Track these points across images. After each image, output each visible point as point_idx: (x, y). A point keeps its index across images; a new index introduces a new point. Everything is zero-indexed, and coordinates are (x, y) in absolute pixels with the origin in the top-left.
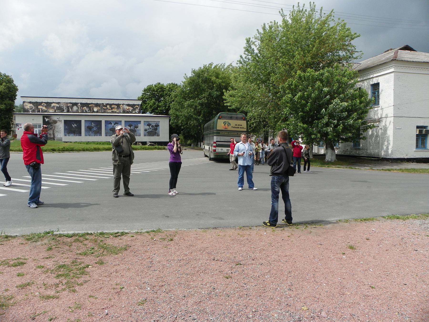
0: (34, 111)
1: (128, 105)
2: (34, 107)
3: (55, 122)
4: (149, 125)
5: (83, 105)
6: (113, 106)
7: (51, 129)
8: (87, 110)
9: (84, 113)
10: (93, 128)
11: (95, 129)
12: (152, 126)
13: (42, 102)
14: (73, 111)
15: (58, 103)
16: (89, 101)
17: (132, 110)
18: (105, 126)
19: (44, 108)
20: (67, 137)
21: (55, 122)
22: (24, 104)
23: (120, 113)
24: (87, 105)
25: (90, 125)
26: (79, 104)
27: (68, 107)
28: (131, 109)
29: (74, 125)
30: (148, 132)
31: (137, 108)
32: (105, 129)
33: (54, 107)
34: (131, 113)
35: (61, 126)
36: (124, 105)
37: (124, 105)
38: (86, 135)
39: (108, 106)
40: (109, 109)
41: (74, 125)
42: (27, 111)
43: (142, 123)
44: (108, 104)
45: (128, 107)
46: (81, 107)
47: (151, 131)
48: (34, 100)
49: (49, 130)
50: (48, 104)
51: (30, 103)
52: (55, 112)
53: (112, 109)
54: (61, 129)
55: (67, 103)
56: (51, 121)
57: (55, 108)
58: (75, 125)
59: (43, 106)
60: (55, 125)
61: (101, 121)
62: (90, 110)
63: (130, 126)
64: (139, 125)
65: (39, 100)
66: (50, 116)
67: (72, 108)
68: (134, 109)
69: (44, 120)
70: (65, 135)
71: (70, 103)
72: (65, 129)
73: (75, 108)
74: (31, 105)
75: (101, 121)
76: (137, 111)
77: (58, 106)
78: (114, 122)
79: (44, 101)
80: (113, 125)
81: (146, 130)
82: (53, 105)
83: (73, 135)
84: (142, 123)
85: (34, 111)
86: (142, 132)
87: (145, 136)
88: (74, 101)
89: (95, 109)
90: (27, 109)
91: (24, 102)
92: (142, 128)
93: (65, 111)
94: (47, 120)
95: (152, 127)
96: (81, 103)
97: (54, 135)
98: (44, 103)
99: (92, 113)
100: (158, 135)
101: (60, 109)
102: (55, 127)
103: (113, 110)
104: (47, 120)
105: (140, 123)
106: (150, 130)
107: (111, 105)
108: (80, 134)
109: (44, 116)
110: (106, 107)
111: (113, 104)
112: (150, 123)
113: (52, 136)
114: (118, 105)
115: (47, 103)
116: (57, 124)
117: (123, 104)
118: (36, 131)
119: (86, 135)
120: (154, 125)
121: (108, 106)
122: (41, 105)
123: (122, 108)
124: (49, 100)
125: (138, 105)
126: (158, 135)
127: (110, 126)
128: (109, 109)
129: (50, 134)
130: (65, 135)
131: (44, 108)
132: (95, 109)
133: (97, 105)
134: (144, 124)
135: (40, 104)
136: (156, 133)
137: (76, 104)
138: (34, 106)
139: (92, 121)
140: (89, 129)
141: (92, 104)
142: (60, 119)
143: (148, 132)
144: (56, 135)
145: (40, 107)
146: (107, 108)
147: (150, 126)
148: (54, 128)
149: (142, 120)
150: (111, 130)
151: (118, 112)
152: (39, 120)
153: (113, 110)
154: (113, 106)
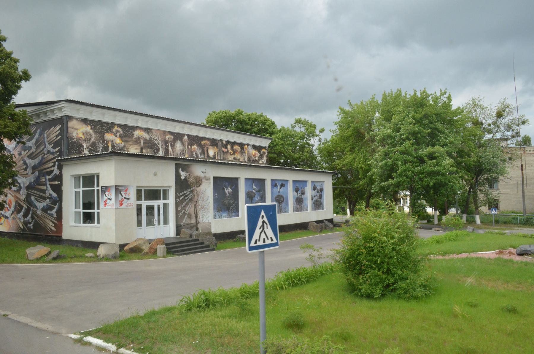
1: (254, 147)
2: (93, 135)
3: (199, 181)
8: (199, 154)
13: (113, 125)
20: (218, 219)
22: (70, 124)
23: (245, 162)
25: (250, 190)
26: (186, 137)
27: (166, 142)
29: (228, 191)
33: (139, 138)
35: (207, 192)
37: (250, 147)
43: (309, 185)
44: (228, 142)
48: (96, 115)
49: (187, 204)
50: (127, 131)
51: (85, 121)
53: (235, 152)
55: (165, 132)
57: (142, 141)
58: (230, 190)
59: (115, 135)
60: (198, 189)
62: (203, 152)
65: (108, 117)
66: (188, 166)
67: (173, 146)
69: (178, 176)
70: (215, 218)
74: (88, 129)
75: (263, 181)
79: (118, 121)
83: (225, 214)
84: (309, 185)
88: (178, 129)
90: (79, 139)
94: (183, 175)
96: (188, 136)
97: (196, 217)
98: (119, 126)
102: (198, 195)
105: (306, 186)
107: (233, 144)
110: (226, 148)
114: (242, 145)
115: (124, 127)
116: (203, 187)
117: (248, 145)
121: (229, 147)
122: (111, 132)
123: (246, 151)
124: (131, 121)
128: (231, 154)
129: (190, 216)
131: (118, 141)
132: (211, 153)
137: (178, 137)
138: (95, 132)
141: (205, 138)
142: (207, 175)
144: (200, 215)
145: (109, 137)
146: (228, 152)
148: (196, 196)
152: (164, 177)
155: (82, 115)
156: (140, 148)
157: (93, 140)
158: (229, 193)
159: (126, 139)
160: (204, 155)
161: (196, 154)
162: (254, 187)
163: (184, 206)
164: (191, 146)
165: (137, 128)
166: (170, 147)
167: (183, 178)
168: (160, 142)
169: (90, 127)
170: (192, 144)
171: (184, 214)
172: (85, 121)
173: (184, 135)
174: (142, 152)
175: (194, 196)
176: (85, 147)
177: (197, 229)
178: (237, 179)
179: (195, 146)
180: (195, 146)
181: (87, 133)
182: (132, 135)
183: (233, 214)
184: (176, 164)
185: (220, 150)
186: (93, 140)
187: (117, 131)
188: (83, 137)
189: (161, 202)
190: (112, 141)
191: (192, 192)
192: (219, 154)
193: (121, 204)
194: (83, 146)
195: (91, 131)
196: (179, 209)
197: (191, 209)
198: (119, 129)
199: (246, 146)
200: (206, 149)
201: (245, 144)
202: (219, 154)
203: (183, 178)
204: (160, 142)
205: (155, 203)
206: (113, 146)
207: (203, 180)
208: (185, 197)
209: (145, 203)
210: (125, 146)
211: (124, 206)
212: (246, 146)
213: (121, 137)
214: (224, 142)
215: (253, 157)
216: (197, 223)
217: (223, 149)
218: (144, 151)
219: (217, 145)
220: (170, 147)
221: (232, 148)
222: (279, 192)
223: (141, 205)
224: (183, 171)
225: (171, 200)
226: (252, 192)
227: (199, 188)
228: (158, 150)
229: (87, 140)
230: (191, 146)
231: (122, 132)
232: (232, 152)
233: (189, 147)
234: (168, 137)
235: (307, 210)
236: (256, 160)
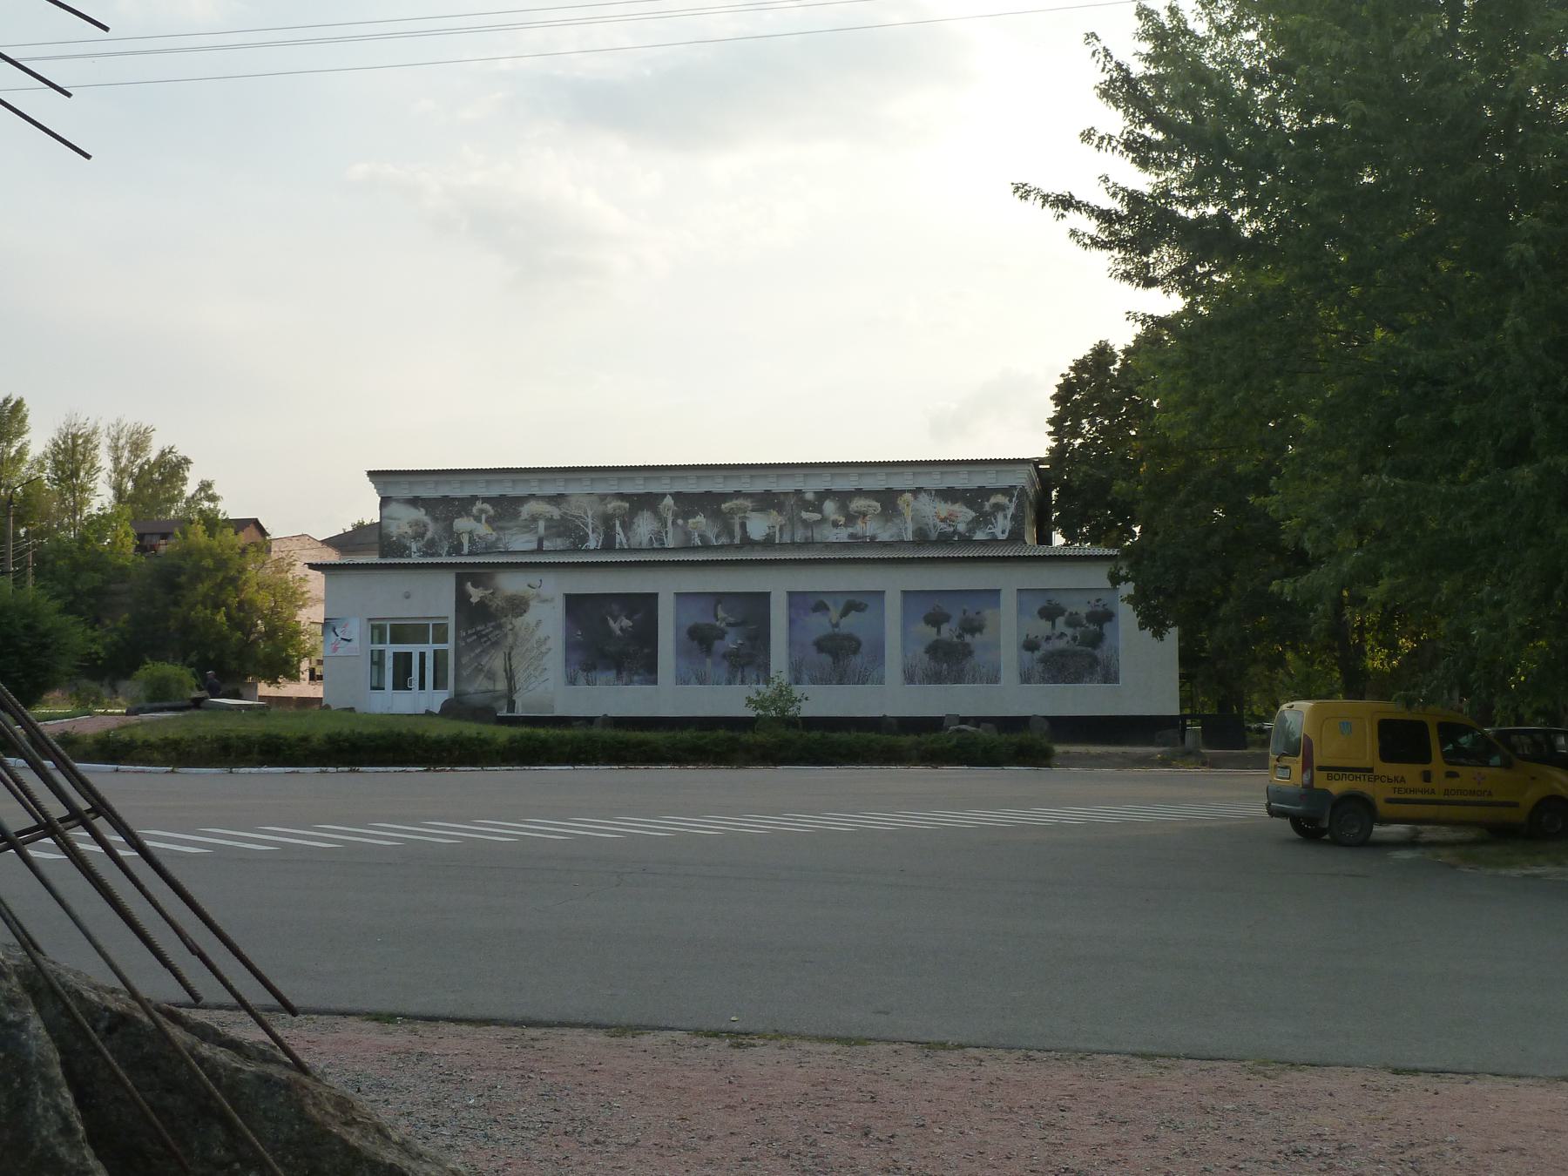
0: (430, 548)
1: (949, 495)
3: (518, 606)
4: (1050, 613)
5: (689, 503)
6: (857, 504)
7: (495, 644)
9: (695, 548)
10: (721, 635)
11: (731, 641)
12: (1073, 622)
13: (474, 499)
14: (634, 543)
15: (557, 499)
16: (718, 486)
17: (975, 524)
18: (791, 622)
19: (483, 529)
20: (582, 688)
21: (518, 606)
24: (708, 503)
26: (669, 501)
27: (607, 521)
28: (963, 514)
30: (1047, 660)
31: (999, 507)
32: (791, 643)
33: (534, 519)
34: (967, 541)
36: (923, 498)
38: (682, 680)
39: (829, 507)
40: (835, 524)
41: (620, 624)
42: (401, 550)
43: (1008, 602)
44: (827, 494)
45: (944, 509)
46: (676, 516)
47: (1062, 653)
50: (506, 507)
52: (540, 550)
53: (851, 519)
54: (550, 644)
55: (603, 498)
56: (498, 602)
57: (542, 524)
58: (626, 623)
60: (518, 622)
61: (763, 598)
63: (935, 620)
64: (988, 613)
67: (627, 526)
68: (983, 519)
69: (462, 598)
70: (572, 681)
71: (622, 496)
72: (570, 646)
73: (645, 527)
74: (420, 514)
75: (763, 598)
76: (1002, 526)
77: (556, 513)
78: (842, 601)
80: (834, 614)
81: (1030, 646)
82: (527, 509)
83: (612, 675)
84: (1008, 602)
85: (430, 548)
86: (1009, 656)
87: (1026, 678)
89: (758, 526)
91: (385, 502)
92: (1008, 628)
93: (592, 544)
94: (476, 594)
95: (1073, 622)
96: (677, 496)
97: (510, 677)
98: (486, 500)
99: (739, 547)
100: (1110, 676)
101: (569, 530)
103: (859, 528)
104: (476, 594)
105: (997, 604)
106: (1061, 644)
107: (843, 497)
108: (648, 669)
109: (467, 575)
111: (859, 492)
112: (1062, 600)
113: (501, 686)
116: (529, 617)
117: (916, 492)
118: (422, 655)
119: (682, 680)
120: (1083, 610)
121: (829, 507)
122: (469, 514)
123: (908, 513)
125: (1007, 491)
126: (1110, 676)
127: (819, 625)
128: (835, 524)
129: (491, 676)
130: (572, 681)
131: (483, 529)
133: (767, 501)
134: (1021, 610)
135: (463, 506)
136: (1095, 661)
137: (648, 502)
138: (435, 519)
139: (719, 598)
140: (700, 639)
143: (1047, 660)
144: (520, 677)
145: (462, 524)
146: (824, 520)
147: (1060, 621)
148: (510, 639)
149: (1008, 581)
150: (820, 646)
151: (884, 536)
153: (859, 528)
154: (857, 504)
155: (409, 494)
156: (534, 538)
157: (429, 535)
158: (621, 629)
159: (500, 524)
160: (732, 536)
161: (702, 537)
162: (721, 614)
163: (479, 656)
164: (686, 519)
165: (533, 496)
166: (618, 529)
167: (474, 600)
168: (590, 521)
169: (423, 511)
170: (687, 515)
171: (479, 669)
172: (414, 502)
173: (664, 495)
174: (540, 550)
175: (506, 635)
176: (414, 549)
177: (512, 705)
178: (654, 597)
179: (700, 519)
180: (700, 519)
181: (417, 523)
182: (517, 515)
183: (636, 678)
184: (458, 575)
185: (791, 520)
186: (429, 535)
187: (482, 511)
188: (410, 531)
189: (429, 649)
190: (470, 533)
191: (500, 627)
192: (787, 530)
193: (335, 649)
194: (409, 548)
195: (427, 519)
196: (465, 660)
197: (497, 662)
198: (487, 506)
199: (908, 496)
200: (737, 521)
201: (903, 492)
202: (787, 530)
203: (474, 600)
204: (590, 521)
205: (414, 649)
206: (471, 541)
207: (532, 603)
208: (480, 637)
209: (390, 649)
210: (498, 539)
211: (340, 652)
212: (908, 496)
213: (490, 521)
214: (810, 496)
215: (943, 525)
216: (511, 689)
217: (805, 515)
218: (547, 545)
219: (780, 508)
220: (618, 529)
221: (843, 508)
222: (836, 625)
223: (381, 652)
224: (475, 586)
225: (450, 646)
226: (713, 627)
227: (520, 619)
228: (585, 538)
229: (419, 536)
230: (686, 519)
231: (492, 512)
232: (842, 520)
233: (680, 522)
234: (612, 505)
235: (995, 679)
236: (955, 532)
